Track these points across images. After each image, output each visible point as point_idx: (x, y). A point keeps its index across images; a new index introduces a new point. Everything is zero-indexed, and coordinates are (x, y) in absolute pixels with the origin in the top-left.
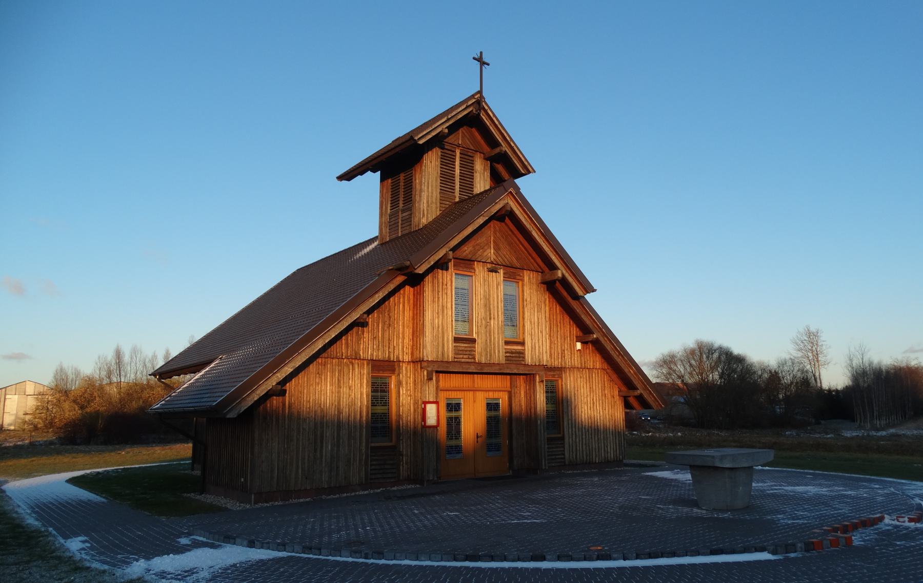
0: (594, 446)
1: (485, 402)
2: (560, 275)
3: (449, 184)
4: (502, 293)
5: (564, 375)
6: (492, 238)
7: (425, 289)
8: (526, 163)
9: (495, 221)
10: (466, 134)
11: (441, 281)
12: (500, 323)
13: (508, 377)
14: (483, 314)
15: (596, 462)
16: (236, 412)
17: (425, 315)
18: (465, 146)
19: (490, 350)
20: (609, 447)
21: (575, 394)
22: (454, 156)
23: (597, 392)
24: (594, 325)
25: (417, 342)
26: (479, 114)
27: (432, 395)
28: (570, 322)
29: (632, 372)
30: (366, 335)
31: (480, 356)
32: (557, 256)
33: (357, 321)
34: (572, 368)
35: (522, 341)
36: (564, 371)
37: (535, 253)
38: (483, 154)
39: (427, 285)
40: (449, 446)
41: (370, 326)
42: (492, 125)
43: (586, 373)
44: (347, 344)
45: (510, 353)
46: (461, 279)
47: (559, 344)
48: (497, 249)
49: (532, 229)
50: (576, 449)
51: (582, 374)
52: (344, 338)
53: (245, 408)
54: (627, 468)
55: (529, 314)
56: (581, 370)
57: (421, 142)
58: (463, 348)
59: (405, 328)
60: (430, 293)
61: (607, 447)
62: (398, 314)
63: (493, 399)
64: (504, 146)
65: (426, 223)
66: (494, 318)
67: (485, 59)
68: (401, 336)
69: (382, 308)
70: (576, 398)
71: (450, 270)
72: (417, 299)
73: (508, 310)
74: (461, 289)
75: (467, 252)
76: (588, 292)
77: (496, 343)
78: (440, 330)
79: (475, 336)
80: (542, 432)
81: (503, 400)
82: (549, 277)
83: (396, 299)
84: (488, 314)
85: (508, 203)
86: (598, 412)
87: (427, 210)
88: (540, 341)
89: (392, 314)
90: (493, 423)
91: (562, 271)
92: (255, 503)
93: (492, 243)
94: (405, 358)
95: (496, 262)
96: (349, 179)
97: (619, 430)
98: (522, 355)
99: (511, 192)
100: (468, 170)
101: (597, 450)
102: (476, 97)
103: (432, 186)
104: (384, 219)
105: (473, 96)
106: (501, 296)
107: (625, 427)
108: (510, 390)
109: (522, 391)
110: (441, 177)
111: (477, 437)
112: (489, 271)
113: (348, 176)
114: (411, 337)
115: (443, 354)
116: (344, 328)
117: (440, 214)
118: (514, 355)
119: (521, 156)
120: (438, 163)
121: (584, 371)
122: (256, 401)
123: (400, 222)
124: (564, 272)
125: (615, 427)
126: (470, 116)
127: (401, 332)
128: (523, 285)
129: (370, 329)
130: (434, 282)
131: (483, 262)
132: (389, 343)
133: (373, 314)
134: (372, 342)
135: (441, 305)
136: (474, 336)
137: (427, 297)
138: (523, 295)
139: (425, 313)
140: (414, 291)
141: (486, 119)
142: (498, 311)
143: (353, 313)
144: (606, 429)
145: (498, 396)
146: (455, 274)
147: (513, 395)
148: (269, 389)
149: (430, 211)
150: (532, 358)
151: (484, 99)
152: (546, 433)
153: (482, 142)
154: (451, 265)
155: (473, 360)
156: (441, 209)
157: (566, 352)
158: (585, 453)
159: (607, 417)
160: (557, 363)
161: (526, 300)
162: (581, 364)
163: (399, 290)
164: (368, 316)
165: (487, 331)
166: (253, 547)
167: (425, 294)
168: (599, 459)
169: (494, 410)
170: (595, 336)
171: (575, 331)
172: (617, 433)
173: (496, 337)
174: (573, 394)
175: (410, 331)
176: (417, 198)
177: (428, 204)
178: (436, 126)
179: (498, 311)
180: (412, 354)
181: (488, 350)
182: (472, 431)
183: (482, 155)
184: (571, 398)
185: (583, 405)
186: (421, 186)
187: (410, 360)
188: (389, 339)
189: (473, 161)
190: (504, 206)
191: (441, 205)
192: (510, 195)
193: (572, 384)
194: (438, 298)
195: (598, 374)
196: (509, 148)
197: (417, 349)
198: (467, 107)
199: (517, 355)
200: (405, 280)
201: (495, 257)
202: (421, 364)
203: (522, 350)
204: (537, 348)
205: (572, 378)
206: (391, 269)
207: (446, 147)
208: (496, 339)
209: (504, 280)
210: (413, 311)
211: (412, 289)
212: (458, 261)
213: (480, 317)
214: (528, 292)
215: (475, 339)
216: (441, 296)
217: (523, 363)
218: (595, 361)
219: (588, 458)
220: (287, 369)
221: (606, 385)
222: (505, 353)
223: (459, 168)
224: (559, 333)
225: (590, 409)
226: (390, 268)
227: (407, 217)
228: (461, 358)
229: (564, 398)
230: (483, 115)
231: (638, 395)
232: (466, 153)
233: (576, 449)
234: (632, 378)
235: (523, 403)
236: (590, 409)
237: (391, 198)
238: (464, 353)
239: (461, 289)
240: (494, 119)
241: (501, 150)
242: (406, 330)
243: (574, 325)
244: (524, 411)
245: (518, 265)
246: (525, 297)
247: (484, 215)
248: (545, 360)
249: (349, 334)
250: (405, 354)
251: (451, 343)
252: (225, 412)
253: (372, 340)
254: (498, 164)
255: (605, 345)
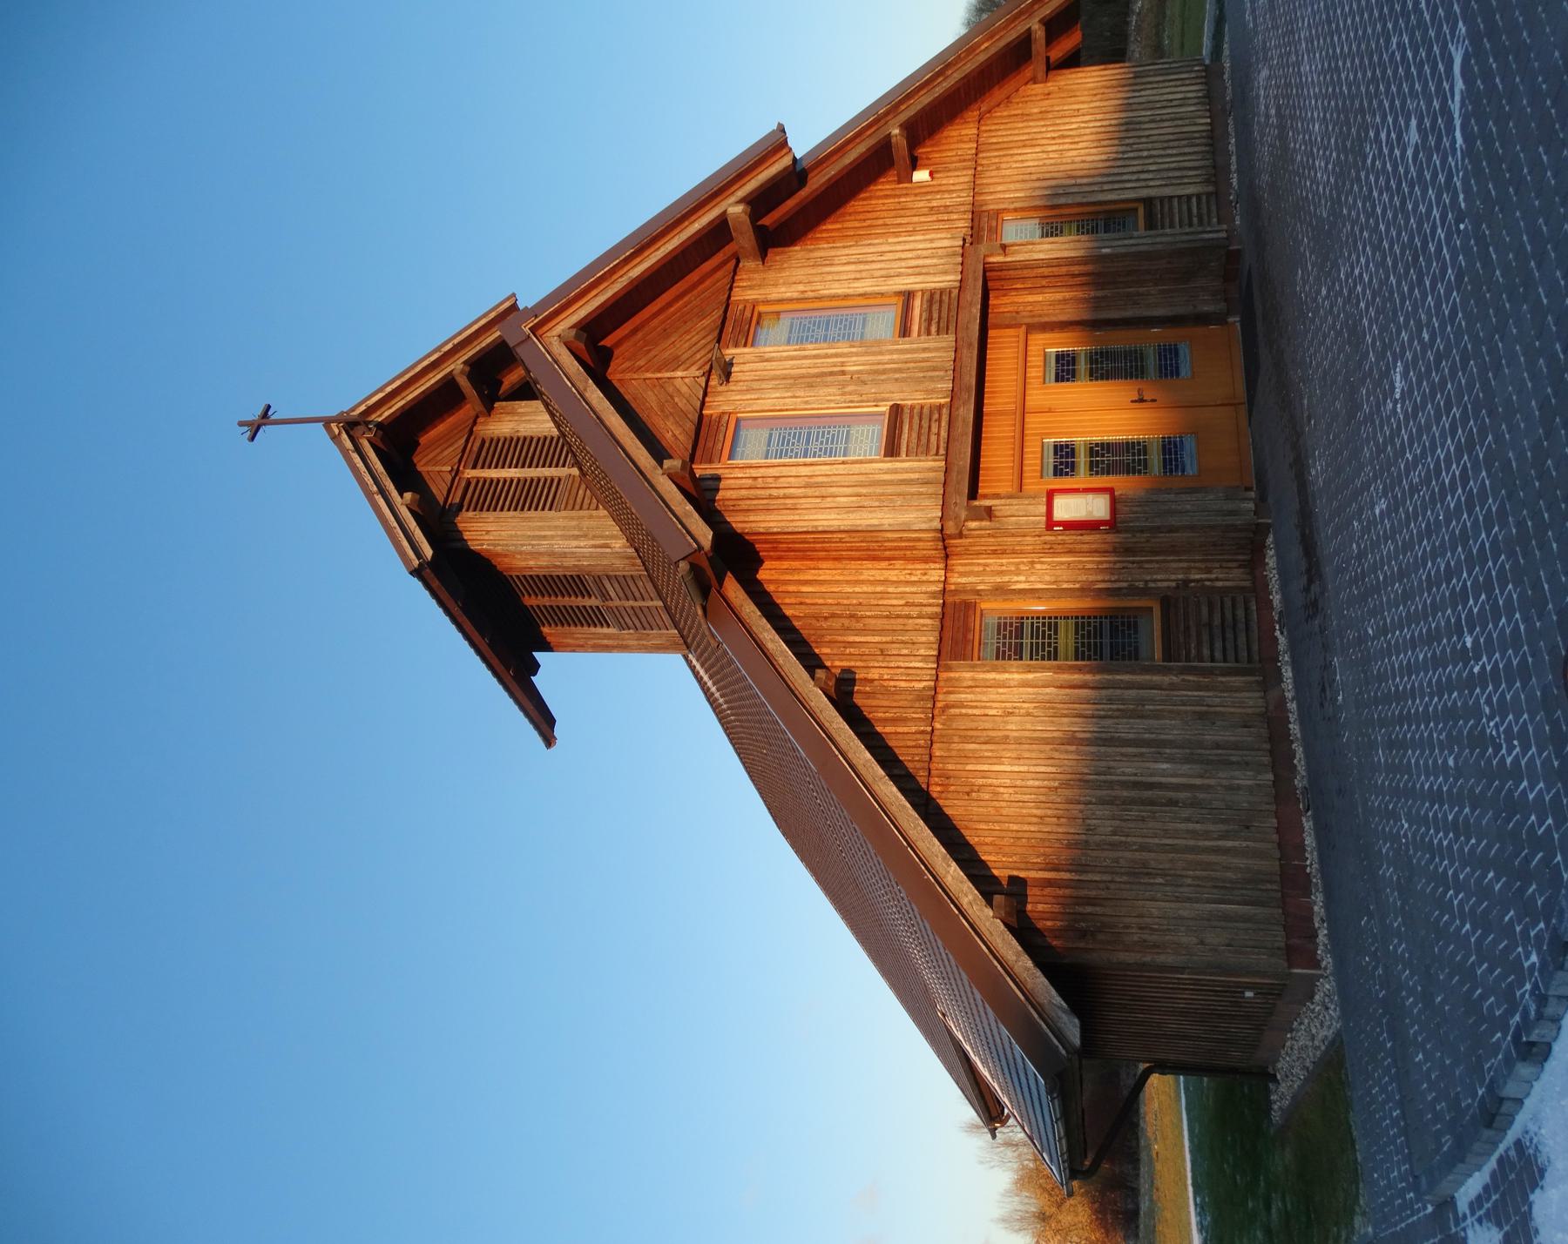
0: (1170, 130)
1: (1054, 384)
2: (739, 209)
3: (539, 490)
4: (781, 349)
5: (991, 207)
6: (649, 375)
7: (761, 530)
8: (493, 315)
9: (609, 370)
10: (430, 456)
11: (744, 492)
12: (854, 350)
13: (991, 333)
14: (832, 390)
15: (1210, 124)
16: (1065, 1017)
17: (826, 529)
18: (456, 460)
19: (922, 370)
20: (1171, 97)
21: (1038, 180)
22: (478, 482)
23: (1035, 130)
24: (870, 135)
25: (895, 549)
26: (379, 426)
27: (1031, 507)
28: (864, 199)
29: (986, 45)
30: (874, 674)
31: (936, 393)
32: (693, 218)
33: (832, 692)
34: (975, 187)
35: (902, 298)
36: (982, 206)
37: (690, 276)
38: (477, 417)
39: (753, 525)
40: (1165, 467)
41: (852, 664)
42: (404, 394)
43: (987, 158)
44: (894, 721)
45: (929, 325)
46: (745, 446)
47: (916, 219)
48: (675, 363)
49: (625, 278)
50: (1174, 169)
51: (988, 165)
52: (879, 729)
53: (1053, 992)
54: (1226, 52)
55: (836, 285)
56: (979, 168)
57: (428, 552)
58: (914, 435)
59: (862, 578)
60: (772, 517)
61: (1171, 100)
62: (827, 595)
63: (1045, 366)
64: (452, 367)
65: (625, 541)
66: (843, 364)
67: (254, 413)
68: (879, 589)
69: (809, 634)
70: (1048, 176)
71: (719, 472)
72: (790, 550)
73: (826, 336)
74: (769, 445)
75: (677, 433)
76: (784, 144)
77: (902, 357)
78: (863, 491)
79: (884, 408)
80: (1132, 242)
81: (1051, 345)
82: (745, 239)
83: (787, 601)
84: (829, 379)
85: (559, 336)
86: (1083, 125)
87: (594, 537)
88: (903, 255)
89: (826, 611)
90: (1105, 367)
91: (730, 205)
92: (1316, 964)
93: (659, 375)
94: (937, 578)
95: (706, 363)
96: (551, 721)
97: (1131, 75)
98: (937, 297)
99: (533, 330)
100: (512, 450)
101: (1180, 122)
102: (337, 431)
103: (541, 528)
104: (631, 643)
105: (335, 438)
106: (791, 351)
107: (1122, 65)
108: (1024, 327)
109: (1026, 300)
110: (522, 509)
111: (1141, 400)
112: (728, 381)
113: (543, 721)
114: (884, 564)
115: (926, 482)
116: (847, 727)
117: (605, 508)
118: (935, 315)
119: (476, 327)
120: (491, 515)
121: (984, 162)
122: (1038, 964)
123: (631, 603)
124: (733, 199)
125: (1124, 86)
126: (381, 445)
127: (870, 589)
128: (767, 302)
129: (858, 664)
130: (746, 507)
131: (705, 394)
132: (898, 617)
133: (823, 657)
134: (892, 658)
135: (803, 490)
136: (884, 409)
137: (783, 524)
138: (791, 300)
139: (820, 529)
140: (772, 558)
141: (390, 408)
142: (827, 356)
143: (812, 704)
144: (1127, 107)
145: (1039, 356)
146: (729, 459)
147: (1036, 320)
148: (1002, 927)
149: (598, 533)
150: (945, 273)
151: (342, 413)
152: (1135, 234)
153: (451, 420)
154: (701, 470)
155: (945, 411)
156: (594, 505)
157: (934, 204)
158: (1187, 150)
159: (1098, 104)
160: (962, 224)
161: (803, 292)
162: (965, 168)
163: (767, 593)
164: (823, 667)
165: (872, 380)
166: (1549, 1047)
167: (775, 530)
168: (1200, 117)
169: (1074, 364)
170: (896, 131)
171: (885, 186)
172: (1137, 81)
173: (887, 357)
174: (1037, 184)
175: (870, 566)
176: (570, 562)
177: (582, 536)
178: (392, 519)
179: (827, 356)
180: (926, 560)
181: (922, 375)
182: (1126, 415)
183: (481, 420)
184: (1046, 188)
185: (1064, 161)
186: (541, 554)
187: (942, 566)
188: (887, 617)
189: (492, 440)
190: (566, 344)
191: (585, 506)
192: (540, 332)
193: (1012, 186)
194: (785, 497)
195: (990, 131)
196: (457, 357)
197: (914, 548)
198: (358, 450)
199: (935, 307)
200: (739, 581)
201: (694, 368)
202: (952, 537)
203: (923, 296)
204: (920, 262)
205: (1000, 188)
206: (704, 609)
207: (457, 500)
208: (895, 357)
209: (752, 345)
210: (819, 559)
211: (767, 564)
212: (699, 453)
213: (838, 398)
214: (783, 289)
215: (892, 406)
216: (782, 492)
217: (955, 292)
218: (959, 138)
219: (1198, 141)
220: (949, 878)
221: (1019, 112)
222: (929, 333)
223: (506, 469)
224: (888, 221)
225: (1077, 143)
226: (700, 612)
227: (616, 585)
228: (938, 440)
229: (1049, 203)
230: (380, 416)
231: (1044, 28)
232: (474, 456)
233: (1174, 169)
234: (1002, 43)
235: (1059, 296)
236: (1077, 143)
237: (595, 626)
238: (925, 430)
239: (769, 445)
240: (389, 389)
241: (462, 372)
242: (866, 575)
243: (872, 188)
244: (1080, 294)
245: (718, 313)
246: (795, 295)
247: (581, 388)
248: (947, 241)
249: (871, 716)
250: (924, 578)
251: (898, 465)
252: (1064, 1052)
253: (888, 658)
254: (501, 383)
255: (919, 107)
